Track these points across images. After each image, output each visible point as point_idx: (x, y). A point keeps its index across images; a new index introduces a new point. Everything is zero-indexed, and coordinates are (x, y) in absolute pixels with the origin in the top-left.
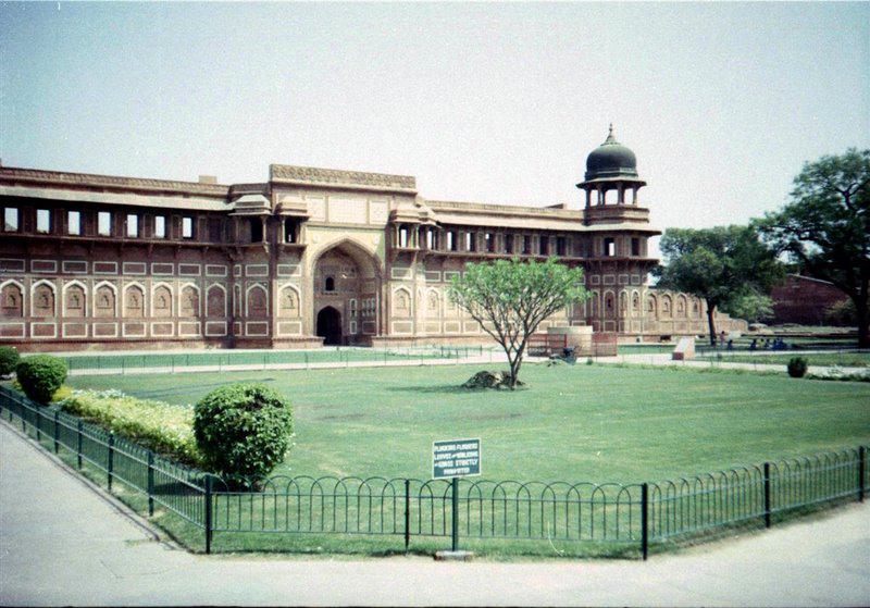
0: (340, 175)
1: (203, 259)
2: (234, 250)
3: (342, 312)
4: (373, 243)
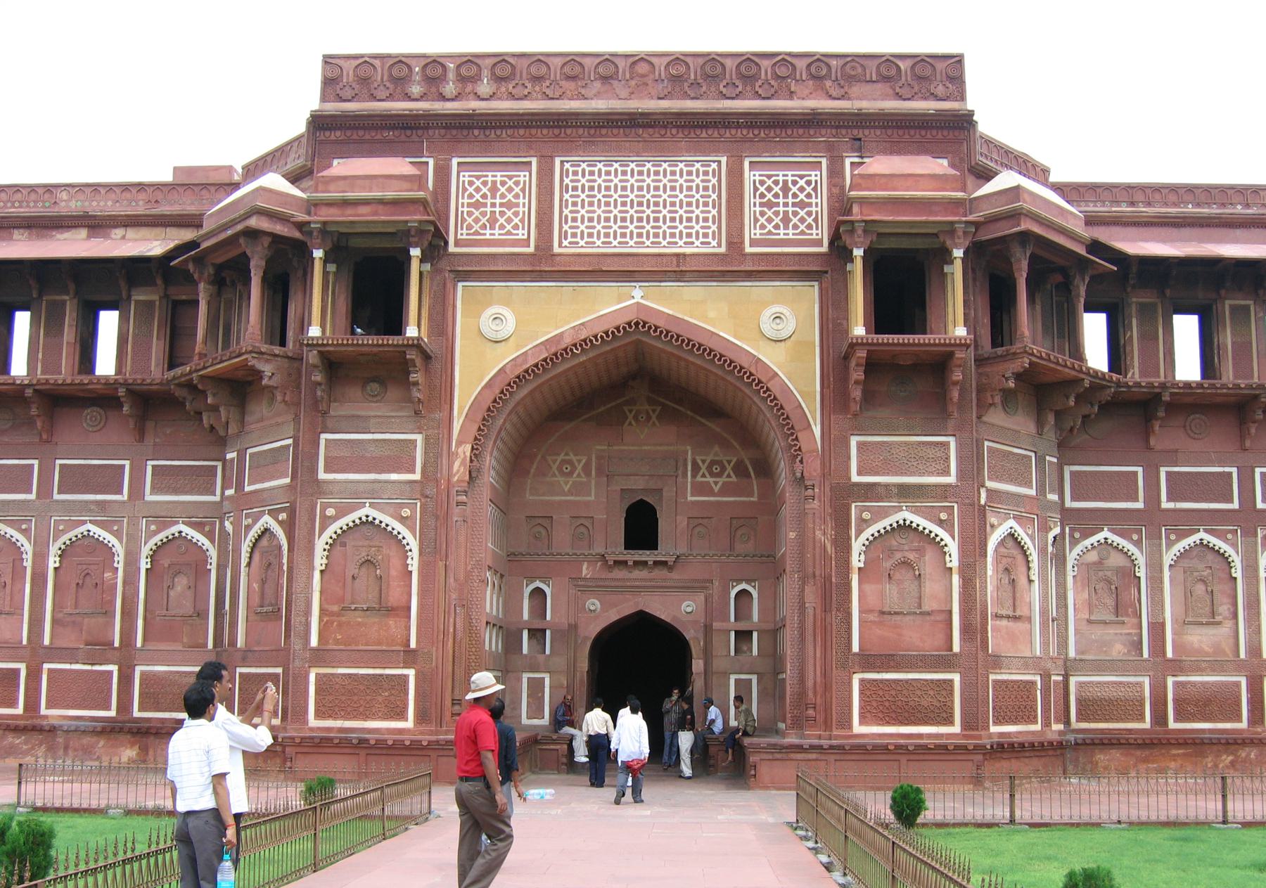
0: (608, 68)
1: (141, 434)
2: (190, 386)
3: (688, 635)
4: (776, 335)
